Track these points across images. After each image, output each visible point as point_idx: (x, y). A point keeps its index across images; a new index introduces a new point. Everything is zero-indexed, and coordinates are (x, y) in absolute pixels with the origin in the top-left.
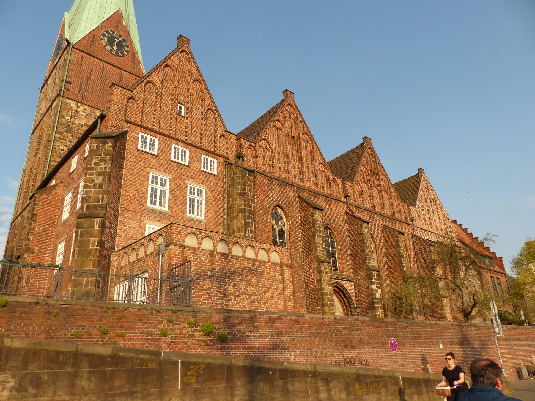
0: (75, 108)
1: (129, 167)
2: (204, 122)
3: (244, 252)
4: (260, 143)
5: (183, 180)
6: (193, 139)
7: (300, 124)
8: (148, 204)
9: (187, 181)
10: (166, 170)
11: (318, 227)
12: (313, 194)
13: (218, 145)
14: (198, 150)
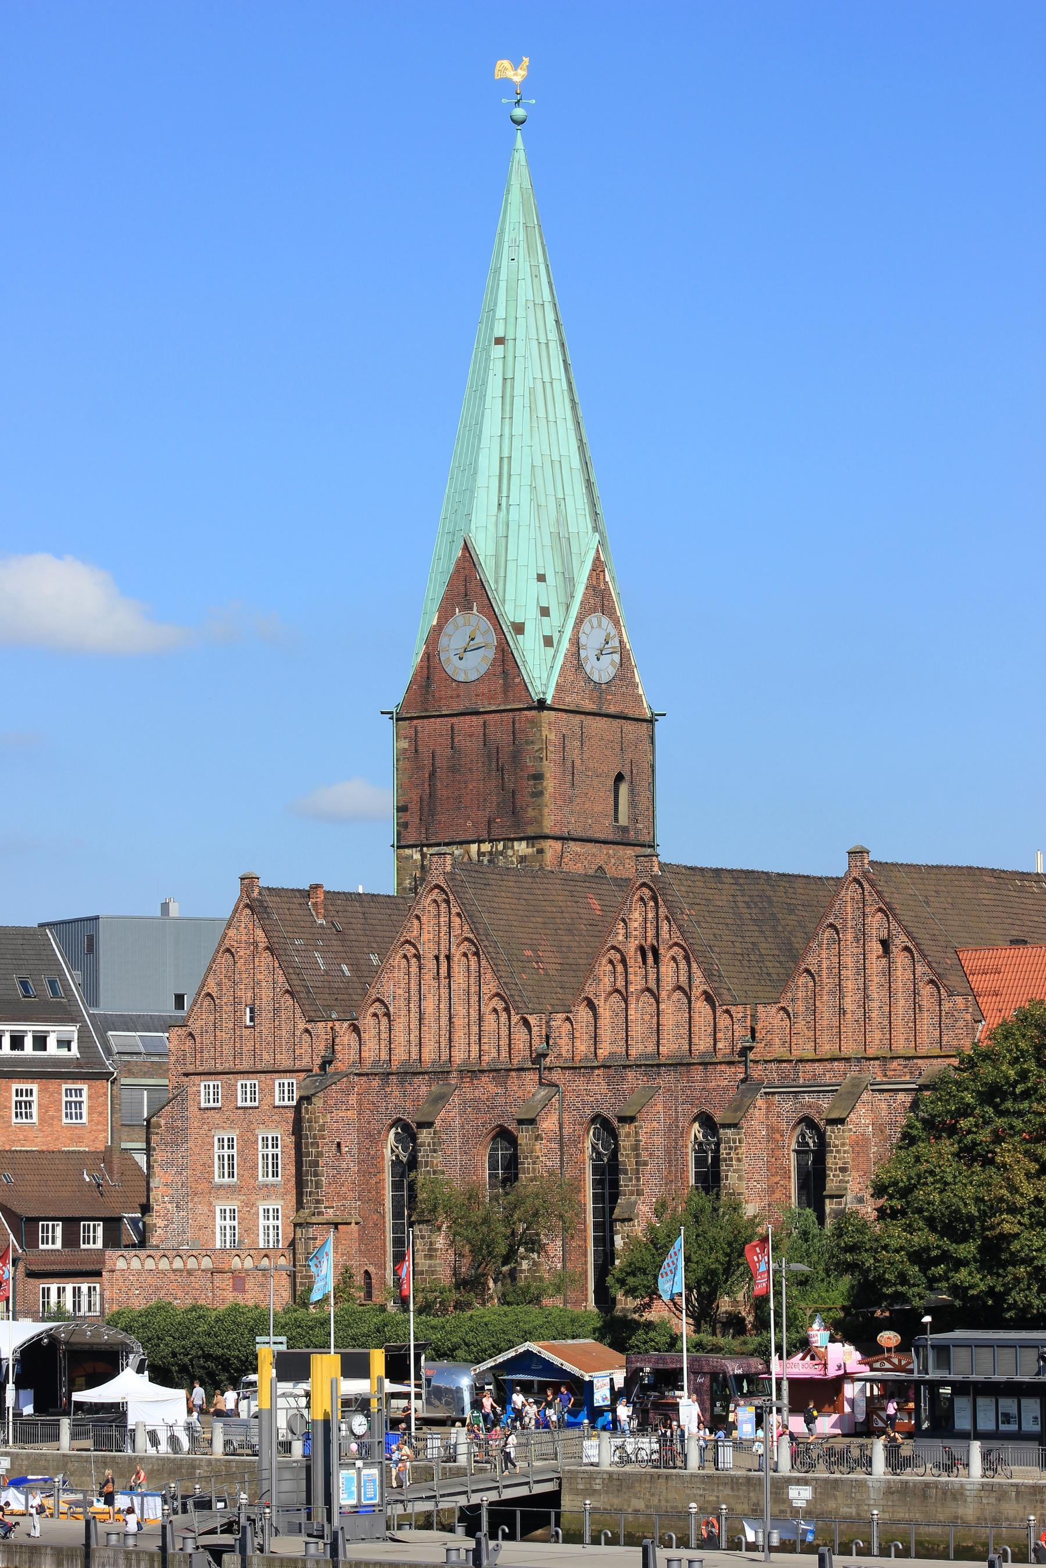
0: (417, 856)
1: (194, 1136)
2: (277, 1023)
3: (171, 1263)
4: (372, 1010)
5: (252, 1131)
6: (266, 1056)
7: (458, 920)
8: (217, 1179)
9: (257, 1132)
10: (232, 1124)
11: (423, 1156)
12: (469, 1074)
13: (297, 1052)
14: (269, 1076)
